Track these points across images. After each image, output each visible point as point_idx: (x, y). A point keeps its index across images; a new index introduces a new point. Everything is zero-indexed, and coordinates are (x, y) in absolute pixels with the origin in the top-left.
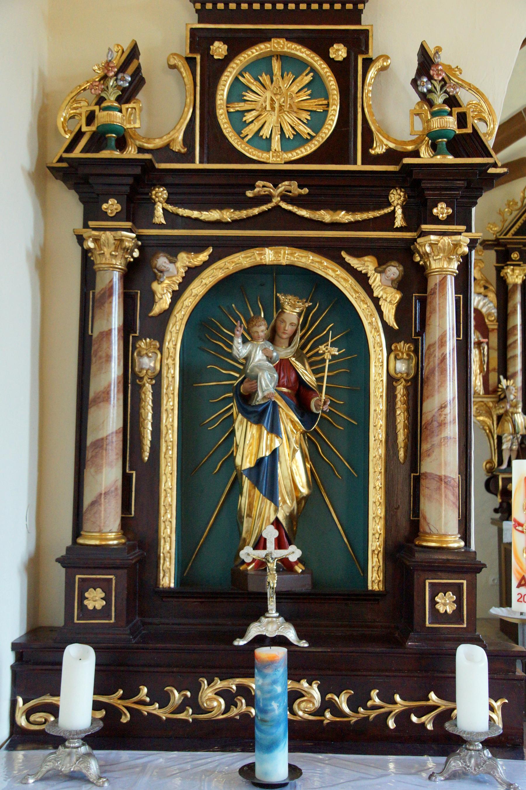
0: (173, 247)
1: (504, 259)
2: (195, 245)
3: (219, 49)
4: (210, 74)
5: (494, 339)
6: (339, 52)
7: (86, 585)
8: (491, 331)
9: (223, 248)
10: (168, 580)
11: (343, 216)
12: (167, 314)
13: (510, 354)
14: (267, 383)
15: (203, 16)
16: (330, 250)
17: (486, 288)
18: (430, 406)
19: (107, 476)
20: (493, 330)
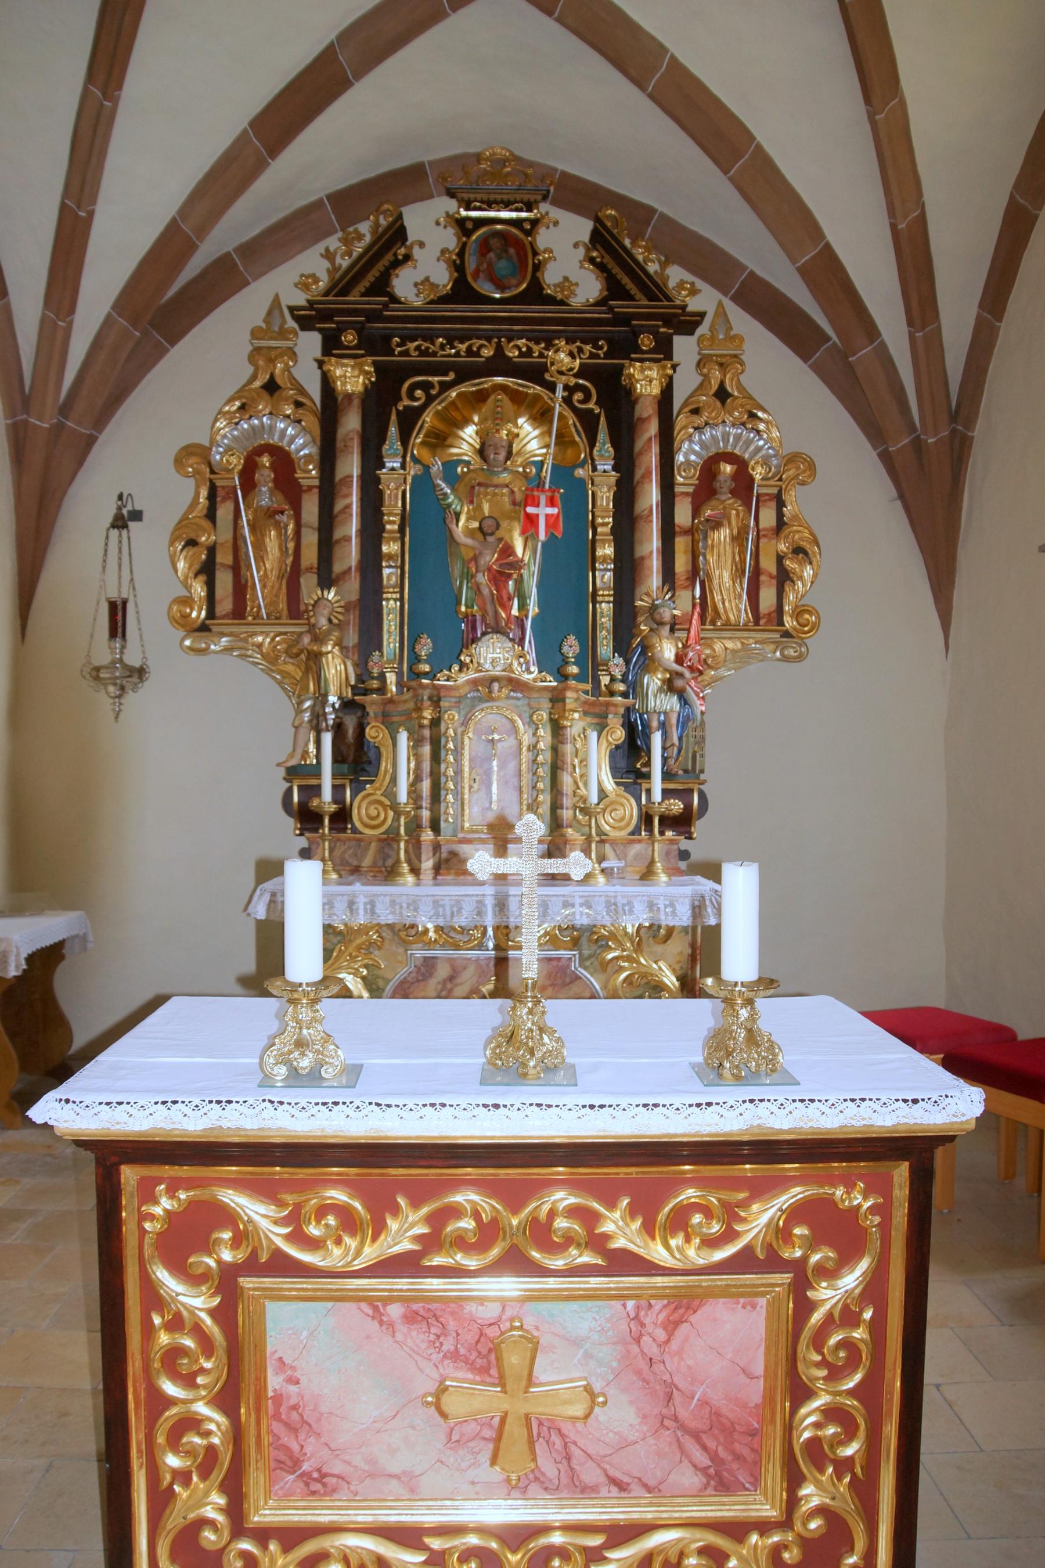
1: (331, 345)
8: (305, 491)
13: (337, 534)
17: (298, 405)
20: (310, 488)
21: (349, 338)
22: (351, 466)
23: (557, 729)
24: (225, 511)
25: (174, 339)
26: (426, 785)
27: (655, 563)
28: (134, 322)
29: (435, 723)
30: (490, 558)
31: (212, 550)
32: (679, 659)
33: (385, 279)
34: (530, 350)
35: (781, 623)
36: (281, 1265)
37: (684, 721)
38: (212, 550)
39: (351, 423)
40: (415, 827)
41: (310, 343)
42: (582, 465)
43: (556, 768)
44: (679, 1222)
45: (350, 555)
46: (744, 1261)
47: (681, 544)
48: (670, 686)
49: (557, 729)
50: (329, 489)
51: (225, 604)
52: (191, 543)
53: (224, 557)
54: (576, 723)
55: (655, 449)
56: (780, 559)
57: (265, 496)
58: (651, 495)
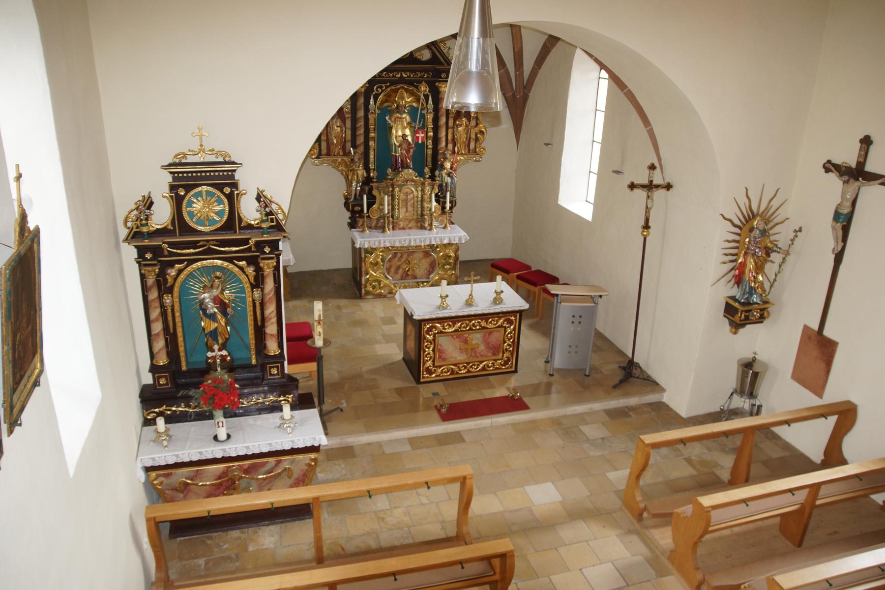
0: (171, 264)
5: (348, 123)
6: (227, 190)
7: (159, 378)
10: (184, 368)
11: (234, 249)
12: (172, 286)
15: (174, 179)
16: (230, 260)
19: (160, 344)
22: (361, 113)
23: (423, 191)
27: (444, 139)
29: (393, 190)
30: (405, 146)
32: (451, 168)
34: (409, 77)
36: (442, 332)
37: (452, 183)
43: (422, 201)
45: (360, 140)
46: (499, 327)
47: (450, 131)
48: (449, 175)
49: (423, 191)
50: (354, 121)
51: (324, 151)
54: (428, 189)
56: (476, 134)
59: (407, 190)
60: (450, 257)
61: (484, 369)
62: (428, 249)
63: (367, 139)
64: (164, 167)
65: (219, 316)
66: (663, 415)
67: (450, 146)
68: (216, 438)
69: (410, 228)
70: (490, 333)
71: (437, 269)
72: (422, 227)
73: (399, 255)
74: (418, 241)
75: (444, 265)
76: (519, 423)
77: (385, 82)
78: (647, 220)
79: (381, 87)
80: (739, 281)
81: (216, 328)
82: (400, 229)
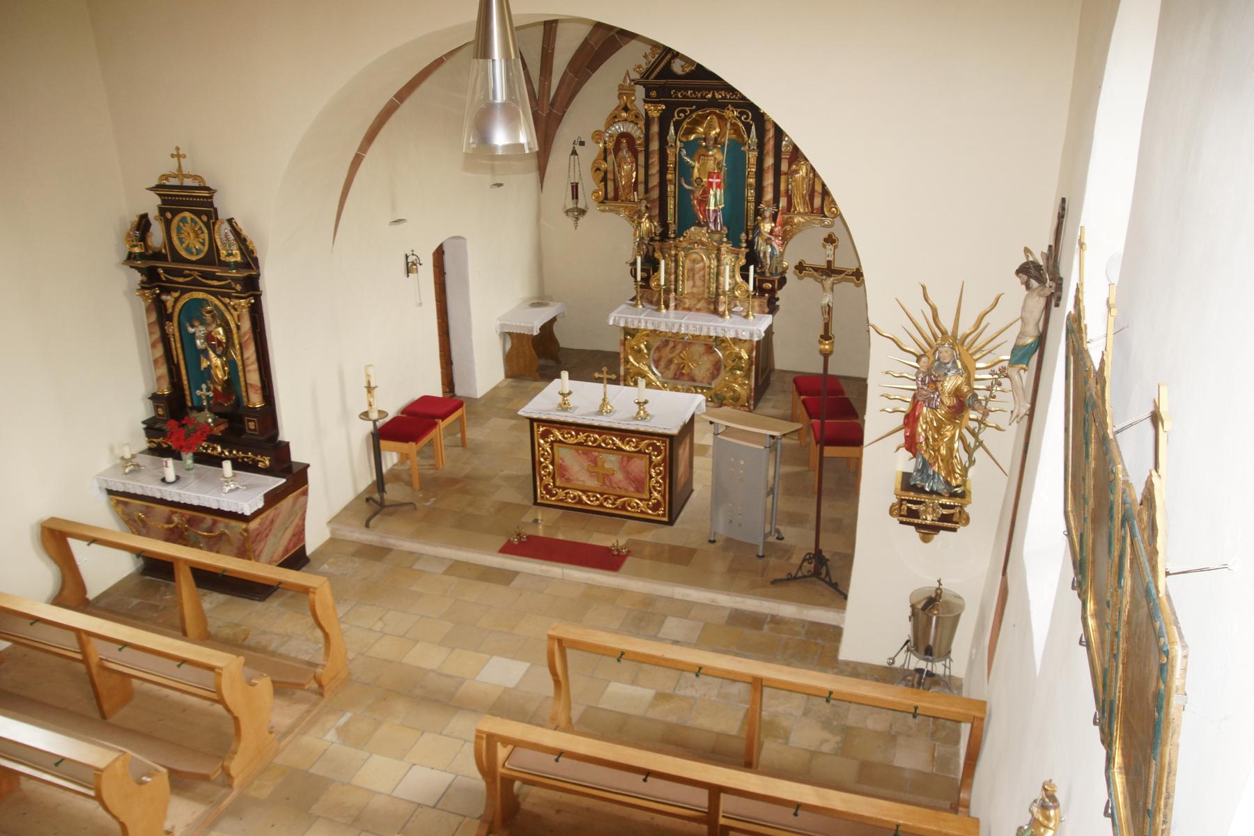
0: (167, 291)
2: (175, 290)
3: (169, 215)
4: (168, 224)
9: (184, 292)
12: (172, 314)
14: (199, 343)
15: (164, 202)
16: (214, 294)
18: (246, 356)
21: (654, 94)
22: (655, 146)
23: (719, 260)
24: (611, 158)
25: (594, 70)
26: (673, 277)
28: (576, 74)
31: (606, 172)
32: (771, 232)
33: (669, 63)
35: (822, 212)
38: (606, 172)
39: (655, 128)
40: (667, 291)
41: (640, 91)
42: (744, 144)
43: (718, 274)
44: (628, 443)
46: (640, 452)
47: (783, 178)
49: (719, 260)
51: (611, 195)
52: (598, 169)
53: (610, 176)
54: (727, 259)
55: (772, 143)
57: (625, 153)
58: (769, 161)
59: (694, 256)
60: (741, 358)
61: (623, 508)
62: (710, 342)
63: (663, 183)
64: (151, 189)
65: (212, 355)
66: (821, 645)
67: (783, 202)
68: (163, 480)
69: (698, 310)
70: (630, 459)
71: (723, 372)
72: (715, 312)
73: (671, 344)
74: (691, 328)
75: (733, 369)
76: (599, 587)
77: (690, 104)
78: (827, 327)
79: (684, 112)
80: (911, 444)
81: (209, 366)
82: (685, 309)
